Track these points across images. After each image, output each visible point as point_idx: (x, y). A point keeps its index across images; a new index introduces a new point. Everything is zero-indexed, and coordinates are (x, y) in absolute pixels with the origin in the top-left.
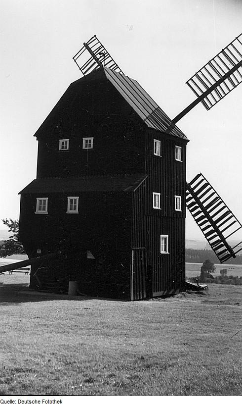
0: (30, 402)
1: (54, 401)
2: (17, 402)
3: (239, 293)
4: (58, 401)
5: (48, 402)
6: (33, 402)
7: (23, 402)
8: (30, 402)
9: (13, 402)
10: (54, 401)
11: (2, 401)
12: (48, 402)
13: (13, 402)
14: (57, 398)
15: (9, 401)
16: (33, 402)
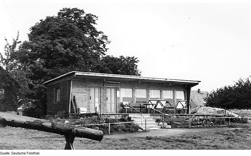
0: (19, 154)
1: (34, 153)
2: (11, 153)
3: (143, 96)
4: (37, 153)
5: (31, 153)
6: (21, 154)
7: (14, 153)
8: (19, 154)
9: (8, 153)
10: (34, 153)
11: (1, 153)
12: (31, 153)
13: (8, 153)
14: (36, 151)
15: (5, 153)
16: (21, 154)
